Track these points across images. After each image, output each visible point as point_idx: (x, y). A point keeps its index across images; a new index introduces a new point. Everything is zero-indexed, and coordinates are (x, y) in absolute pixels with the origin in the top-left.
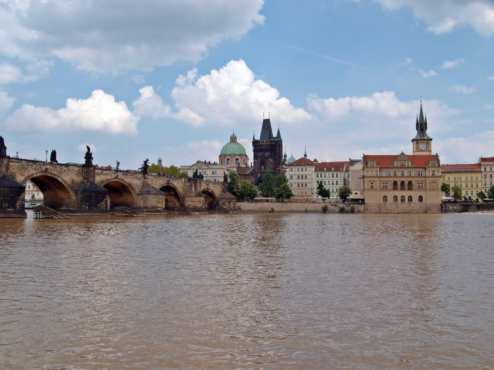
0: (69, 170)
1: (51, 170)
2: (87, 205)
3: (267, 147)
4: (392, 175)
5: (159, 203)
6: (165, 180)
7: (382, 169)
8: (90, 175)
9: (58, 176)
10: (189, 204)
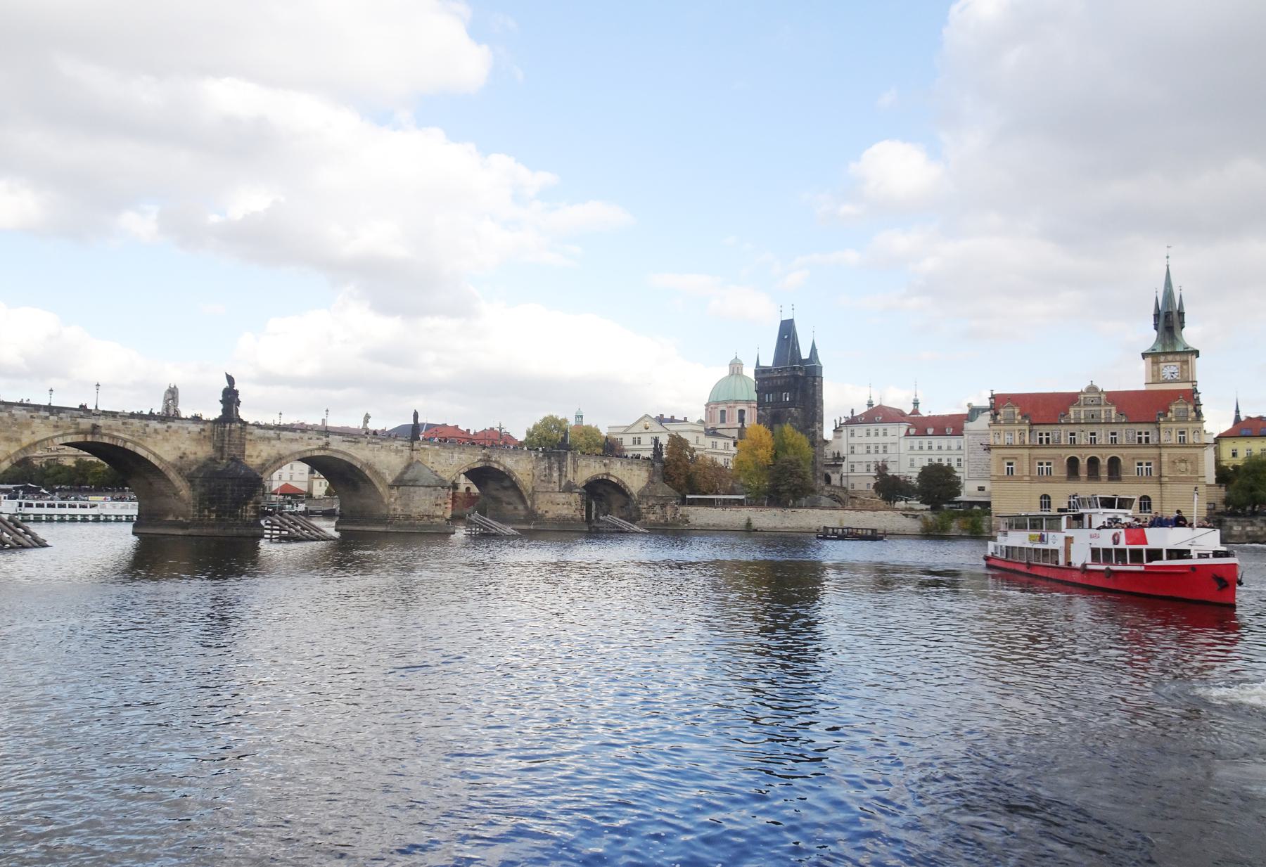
1: (111, 429)
2: (213, 512)
3: (785, 382)
4: (1063, 443)
5: (438, 507)
6: (477, 455)
7: (1035, 427)
9: (136, 444)
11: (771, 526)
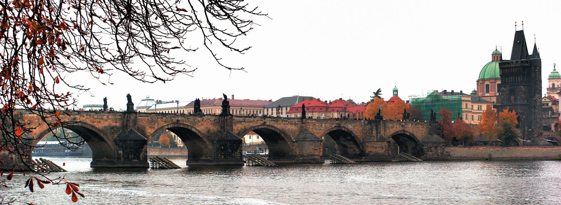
0: (204, 120)
1: (183, 121)
2: (223, 155)
3: (518, 70)
6: (334, 124)
8: (227, 124)
9: (191, 127)
10: (370, 151)
11: (495, 156)
